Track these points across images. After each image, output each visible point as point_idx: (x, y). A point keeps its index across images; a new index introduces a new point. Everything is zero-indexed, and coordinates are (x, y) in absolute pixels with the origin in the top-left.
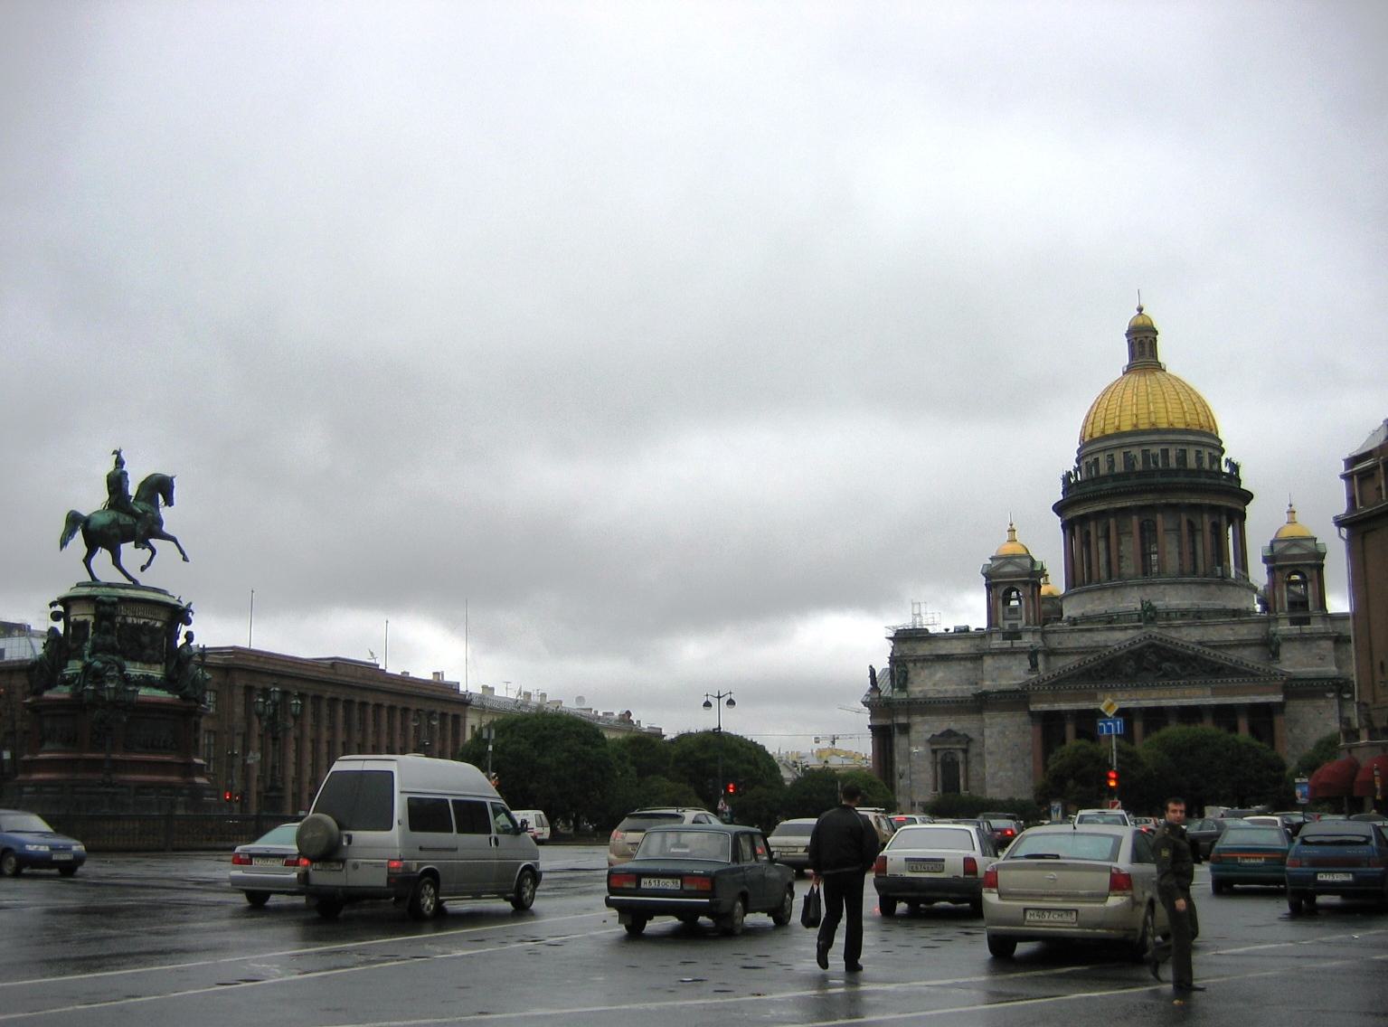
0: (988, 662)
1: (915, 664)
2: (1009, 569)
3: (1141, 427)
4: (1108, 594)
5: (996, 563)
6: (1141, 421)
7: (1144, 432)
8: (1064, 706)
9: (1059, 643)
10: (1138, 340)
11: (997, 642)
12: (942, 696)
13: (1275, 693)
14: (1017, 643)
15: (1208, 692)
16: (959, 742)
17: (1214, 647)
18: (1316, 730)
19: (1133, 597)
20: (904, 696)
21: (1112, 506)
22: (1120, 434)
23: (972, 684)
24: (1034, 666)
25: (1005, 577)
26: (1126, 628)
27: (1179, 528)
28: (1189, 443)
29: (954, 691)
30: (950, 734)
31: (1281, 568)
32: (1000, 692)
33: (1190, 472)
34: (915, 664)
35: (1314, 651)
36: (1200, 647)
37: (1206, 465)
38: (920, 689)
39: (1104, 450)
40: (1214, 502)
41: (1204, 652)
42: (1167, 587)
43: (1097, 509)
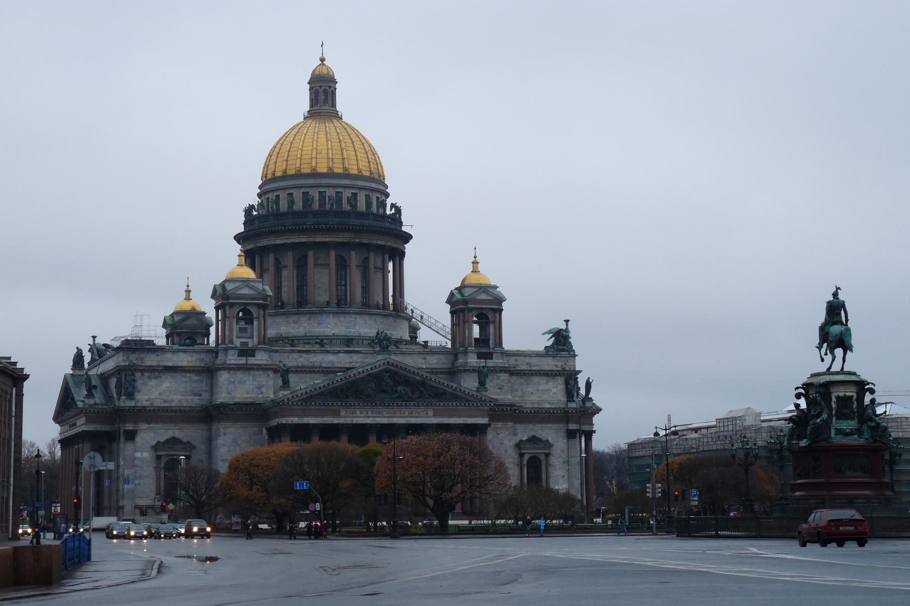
0: (224, 377)
1: (143, 374)
2: (246, 291)
3: (336, 170)
4: (304, 319)
6: (336, 166)
8: (312, 420)
9: (280, 362)
11: (233, 358)
12: (166, 404)
13: (483, 416)
14: (251, 360)
15: (431, 413)
16: (184, 449)
17: (432, 373)
18: (494, 447)
20: (132, 403)
22: (314, 175)
23: (195, 395)
24: (286, 384)
26: (339, 352)
28: (373, 190)
29: (180, 401)
30: (173, 441)
31: (470, 310)
33: (359, 215)
34: (143, 374)
36: (428, 375)
37: (374, 209)
40: (394, 246)
42: (358, 316)
43: (297, 241)
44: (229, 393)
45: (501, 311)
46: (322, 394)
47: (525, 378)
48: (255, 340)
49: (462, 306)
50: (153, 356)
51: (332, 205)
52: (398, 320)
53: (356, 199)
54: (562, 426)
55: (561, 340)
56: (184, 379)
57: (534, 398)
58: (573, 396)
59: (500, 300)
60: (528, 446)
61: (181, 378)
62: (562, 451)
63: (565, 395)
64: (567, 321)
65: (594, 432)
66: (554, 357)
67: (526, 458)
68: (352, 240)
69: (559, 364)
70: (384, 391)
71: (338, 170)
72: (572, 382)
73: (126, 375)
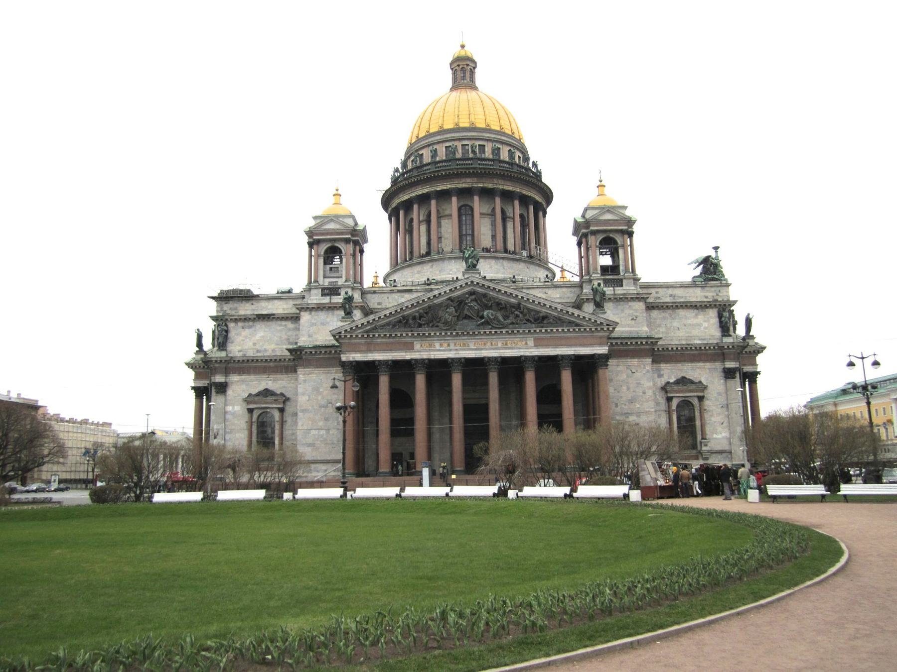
0: (305, 317)
2: (331, 226)
3: (461, 125)
5: (318, 221)
9: (379, 304)
11: (315, 298)
15: (531, 343)
18: (628, 389)
21: (434, 189)
25: (327, 234)
27: (493, 214)
28: (503, 143)
29: (273, 350)
30: (266, 393)
31: (594, 233)
32: (315, 347)
38: (239, 348)
39: (428, 146)
41: (528, 299)
43: (420, 192)
44: (310, 336)
45: (630, 234)
46: (388, 324)
47: (670, 311)
48: (344, 279)
49: (584, 231)
51: (454, 153)
52: (532, 267)
53: (484, 152)
54: (718, 365)
55: (710, 269)
56: (279, 328)
57: (681, 334)
58: (728, 330)
59: (630, 222)
60: (676, 388)
61: (276, 326)
62: (719, 394)
64: (716, 248)
65: (759, 373)
67: (675, 403)
68: (475, 185)
70: (467, 317)
71: (464, 124)
72: (726, 314)
73: (219, 325)
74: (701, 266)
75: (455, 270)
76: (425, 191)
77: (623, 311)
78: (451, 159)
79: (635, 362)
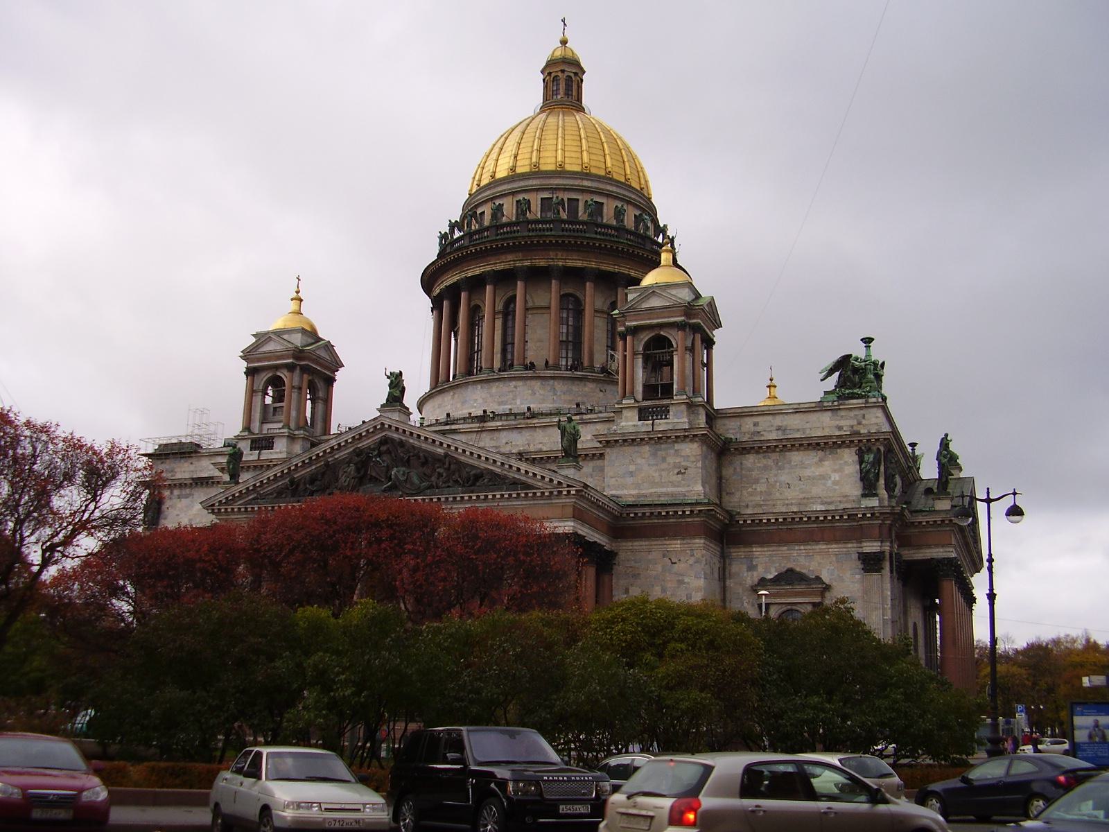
2: (270, 347)
3: (519, 170)
7: (524, 176)
10: (553, 75)
19: (476, 400)
21: (464, 275)
31: (635, 331)
34: (172, 493)
35: (671, 460)
42: (520, 383)
47: (775, 456)
50: (186, 465)
54: (852, 547)
55: (856, 377)
57: (792, 494)
63: (859, 485)
66: (834, 410)
69: (842, 423)
74: (837, 374)
75: (480, 401)
76: (455, 279)
77: (664, 459)
78: (496, 226)
79: (676, 544)
